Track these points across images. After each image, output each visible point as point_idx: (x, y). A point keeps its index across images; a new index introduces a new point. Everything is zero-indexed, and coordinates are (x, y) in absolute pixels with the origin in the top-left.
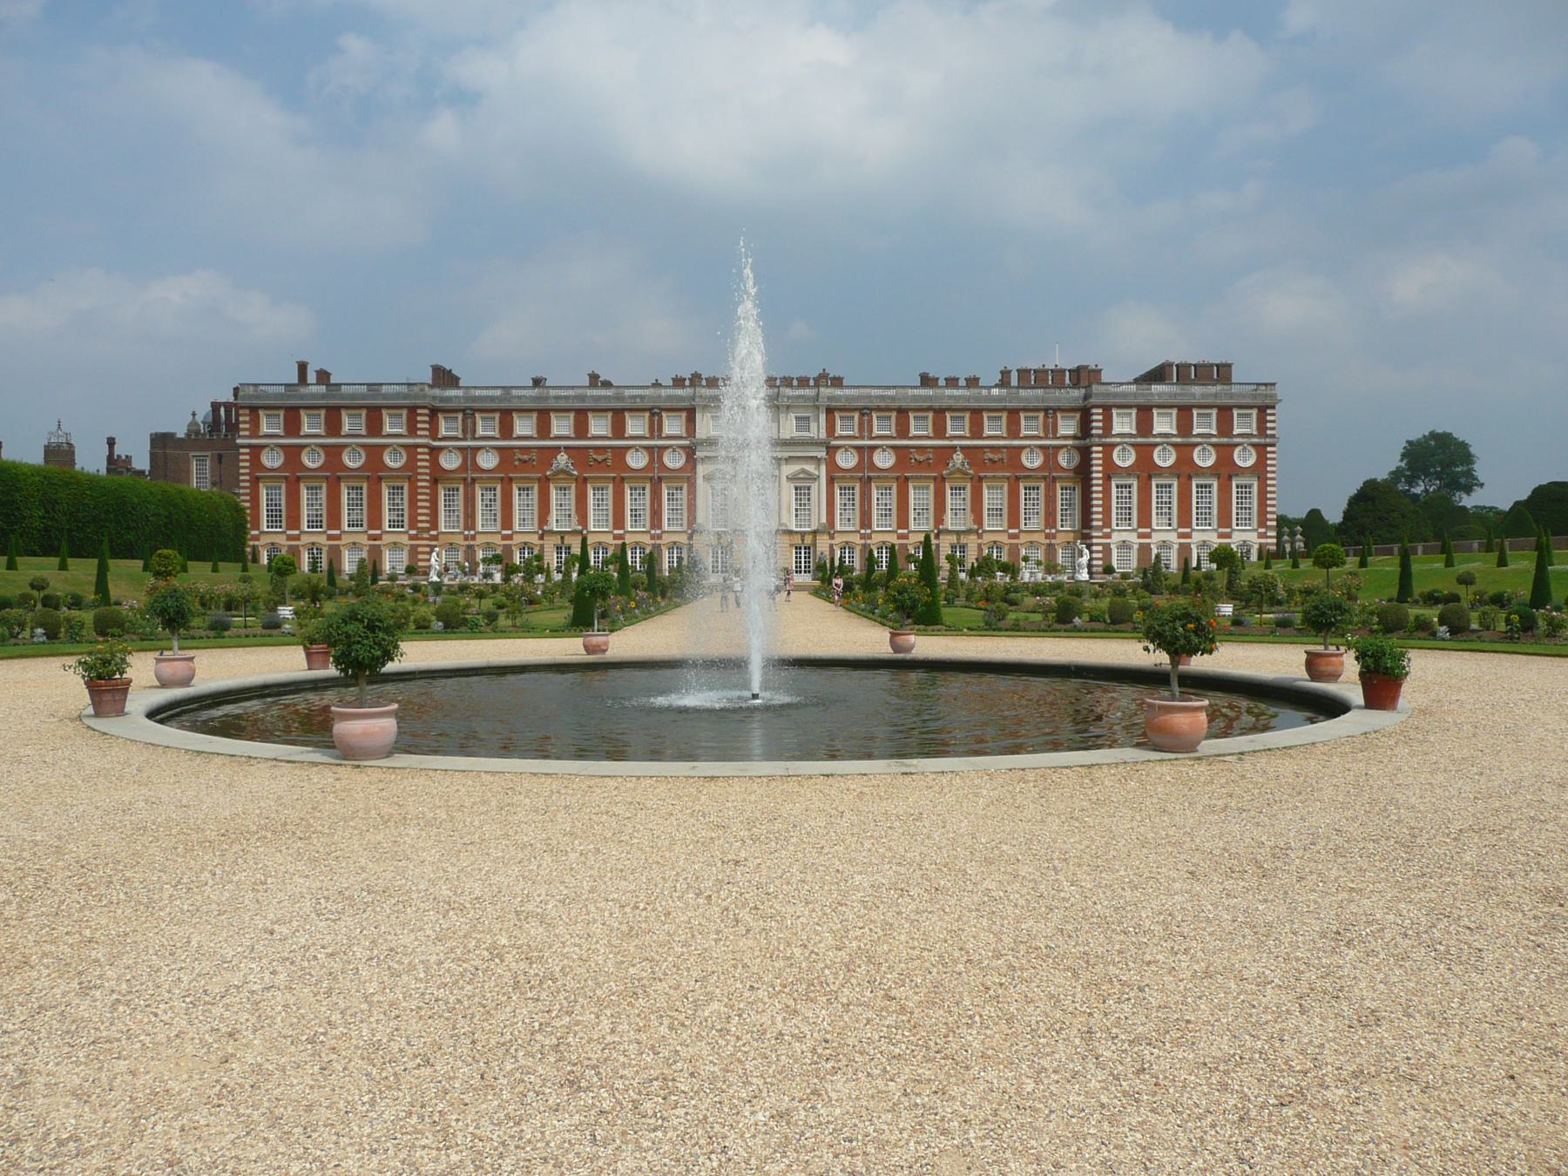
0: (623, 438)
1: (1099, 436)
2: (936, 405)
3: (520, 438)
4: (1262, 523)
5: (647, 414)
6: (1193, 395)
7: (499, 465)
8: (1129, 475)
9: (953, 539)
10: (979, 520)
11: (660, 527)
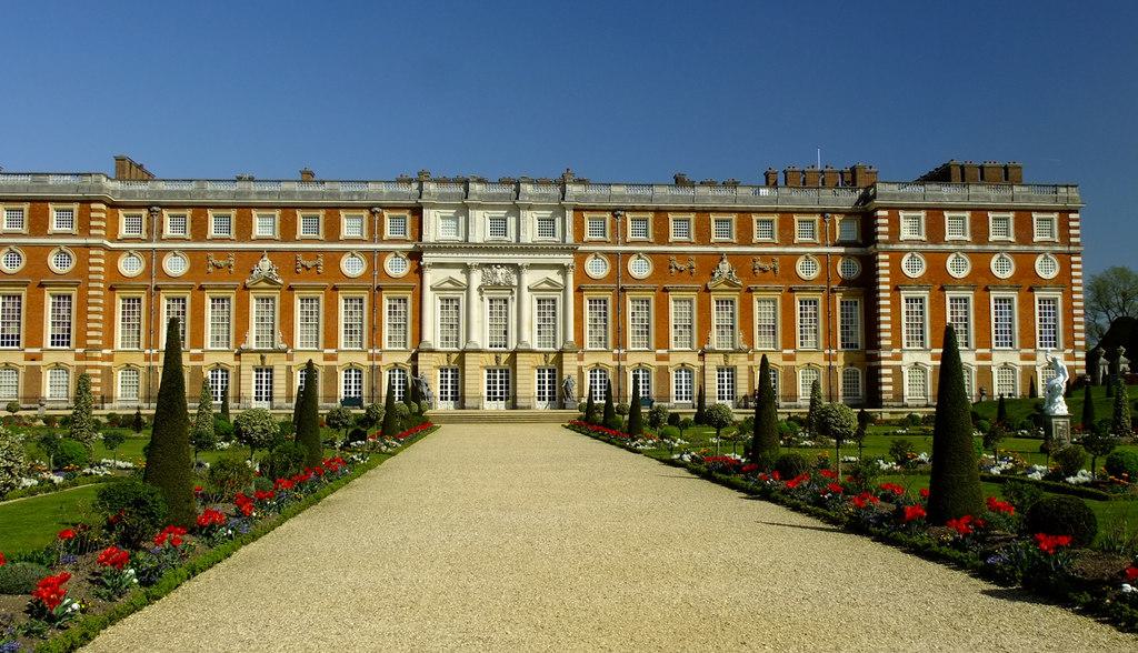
0: (338, 241)
1: (886, 242)
2: (699, 205)
3: (214, 240)
4: (1070, 343)
5: (365, 213)
6: (988, 198)
7: (191, 270)
8: (920, 288)
9: (719, 360)
10: (750, 339)
11: (380, 346)
